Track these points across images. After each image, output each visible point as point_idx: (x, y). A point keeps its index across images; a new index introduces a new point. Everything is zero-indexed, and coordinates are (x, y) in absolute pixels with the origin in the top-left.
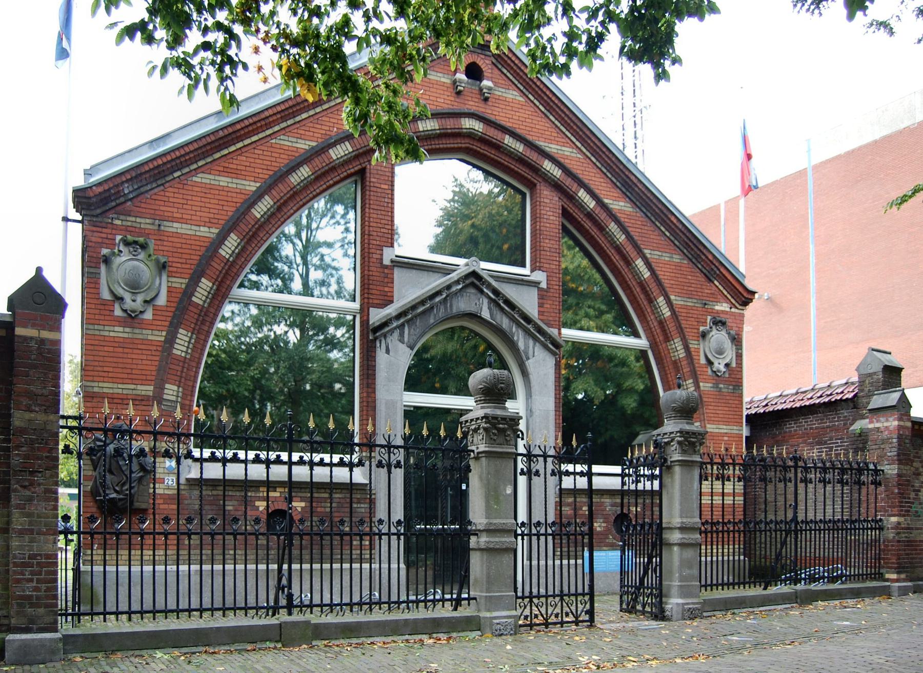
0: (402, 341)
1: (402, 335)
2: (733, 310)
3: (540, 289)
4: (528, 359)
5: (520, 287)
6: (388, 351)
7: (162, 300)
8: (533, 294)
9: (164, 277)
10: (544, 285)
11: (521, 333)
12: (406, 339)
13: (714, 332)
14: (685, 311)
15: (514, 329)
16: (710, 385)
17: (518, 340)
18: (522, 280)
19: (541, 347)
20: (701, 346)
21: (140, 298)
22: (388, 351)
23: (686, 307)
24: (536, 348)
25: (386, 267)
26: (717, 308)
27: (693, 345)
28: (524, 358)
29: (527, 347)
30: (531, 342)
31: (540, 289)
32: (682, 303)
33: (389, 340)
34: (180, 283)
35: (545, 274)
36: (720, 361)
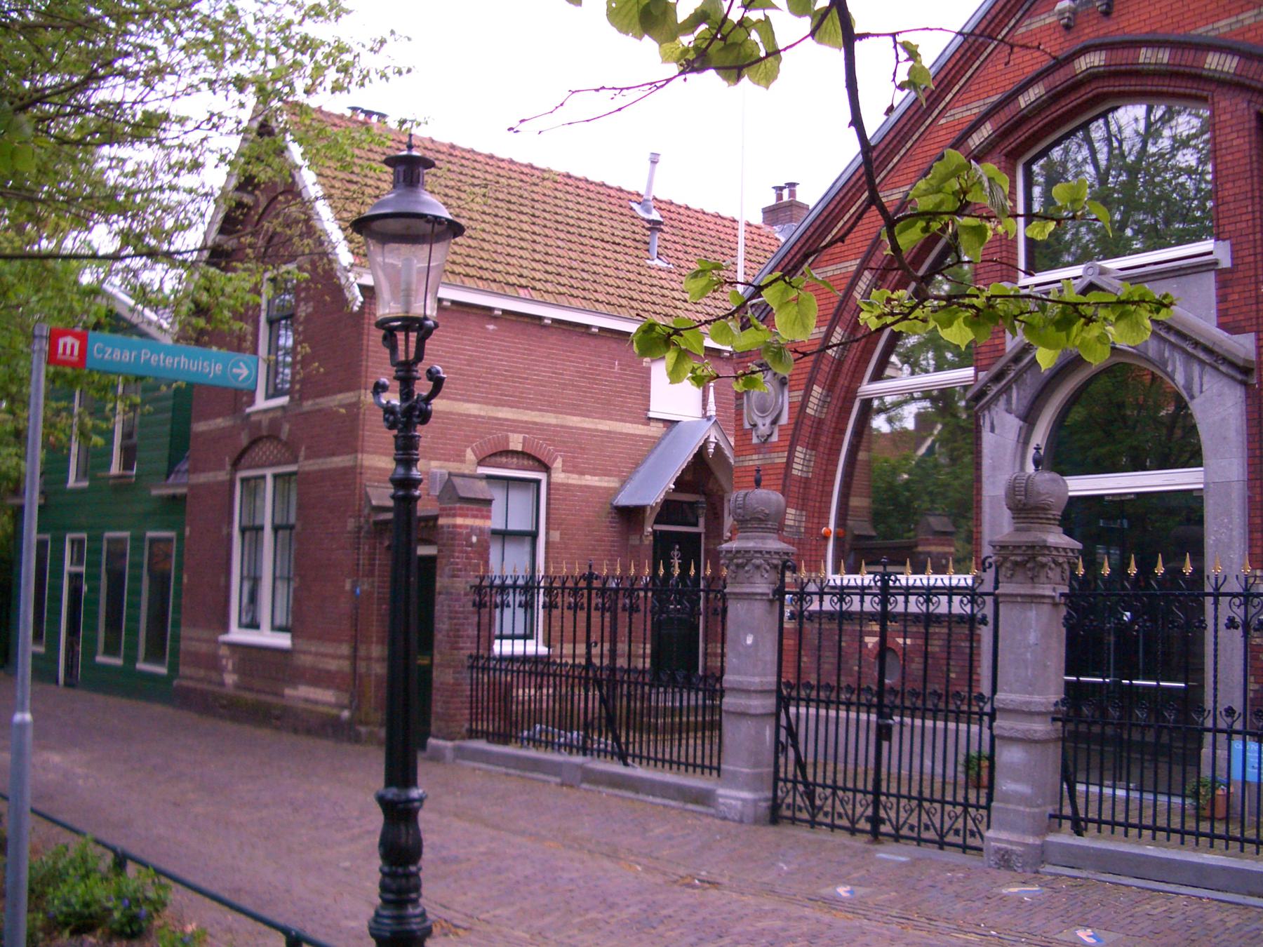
0: (1009, 411)
1: (1009, 401)
3: (1221, 273)
4: (1192, 397)
5: (1184, 279)
6: (992, 430)
7: (784, 420)
8: (1207, 284)
9: (786, 393)
10: (1226, 263)
12: (1014, 406)
15: (1167, 354)
17: (1174, 371)
18: (1180, 269)
19: (1214, 373)
21: (768, 421)
22: (992, 430)
24: (1205, 379)
28: (1187, 398)
30: (1196, 369)
31: (1221, 273)
33: (993, 412)
34: (798, 395)
35: (1227, 243)
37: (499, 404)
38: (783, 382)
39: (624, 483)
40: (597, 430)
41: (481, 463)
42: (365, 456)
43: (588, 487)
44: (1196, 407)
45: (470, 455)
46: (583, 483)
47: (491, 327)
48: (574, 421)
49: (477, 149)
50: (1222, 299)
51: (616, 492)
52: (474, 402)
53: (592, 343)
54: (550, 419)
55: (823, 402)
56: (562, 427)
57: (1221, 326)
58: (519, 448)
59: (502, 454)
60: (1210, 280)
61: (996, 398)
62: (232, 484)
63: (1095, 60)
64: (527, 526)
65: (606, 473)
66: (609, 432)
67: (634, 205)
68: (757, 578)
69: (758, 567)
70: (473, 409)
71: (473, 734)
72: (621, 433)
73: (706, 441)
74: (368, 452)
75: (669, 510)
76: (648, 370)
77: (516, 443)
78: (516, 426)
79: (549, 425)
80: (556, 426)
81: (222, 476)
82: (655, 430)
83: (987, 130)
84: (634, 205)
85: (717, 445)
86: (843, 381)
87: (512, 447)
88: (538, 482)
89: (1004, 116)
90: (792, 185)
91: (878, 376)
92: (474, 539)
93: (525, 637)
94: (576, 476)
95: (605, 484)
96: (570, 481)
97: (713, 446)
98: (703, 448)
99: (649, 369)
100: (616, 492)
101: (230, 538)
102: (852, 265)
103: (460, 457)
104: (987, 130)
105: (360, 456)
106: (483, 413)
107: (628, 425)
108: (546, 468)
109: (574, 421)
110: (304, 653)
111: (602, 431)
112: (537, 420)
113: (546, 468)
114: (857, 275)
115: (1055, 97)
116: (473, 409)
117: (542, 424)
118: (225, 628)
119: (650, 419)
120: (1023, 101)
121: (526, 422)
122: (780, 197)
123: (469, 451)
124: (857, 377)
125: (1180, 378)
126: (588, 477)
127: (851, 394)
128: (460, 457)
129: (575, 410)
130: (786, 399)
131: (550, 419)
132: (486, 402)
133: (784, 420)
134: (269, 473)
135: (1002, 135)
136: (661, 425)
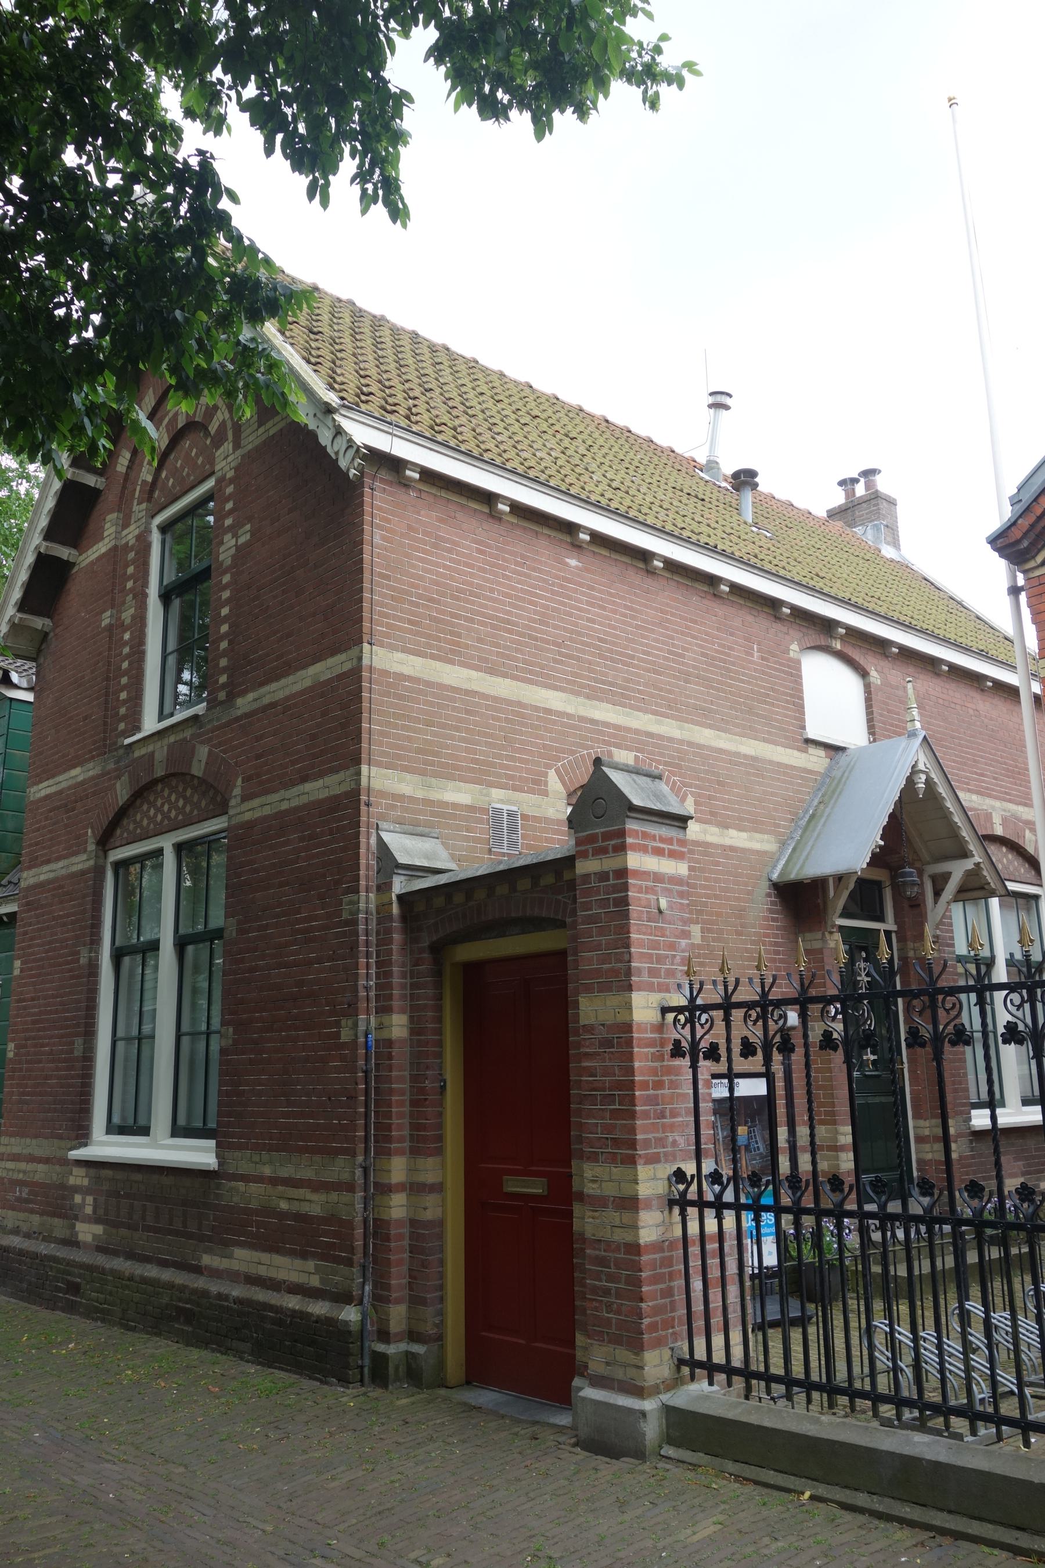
37: (594, 695)
40: (737, 754)
42: (374, 770)
43: (732, 848)
46: (728, 842)
47: (573, 562)
48: (706, 736)
52: (555, 688)
53: (720, 610)
54: (669, 728)
56: (690, 744)
62: (98, 872)
65: (755, 826)
66: (754, 759)
70: (555, 700)
72: (771, 762)
73: (914, 771)
74: (379, 765)
79: (671, 739)
80: (681, 742)
81: (80, 862)
85: (929, 782)
90: (869, 474)
94: (714, 829)
95: (757, 846)
96: (710, 839)
97: (923, 777)
98: (910, 781)
99: (799, 662)
101: (93, 970)
105: (364, 768)
106: (570, 710)
107: (780, 749)
109: (706, 736)
110: (245, 1178)
111: (745, 756)
112: (654, 728)
116: (555, 700)
117: (660, 737)
118: (82, 1135)
119: (808, 741)
121: (637, 732)
122: (850, 493)
123: (552, 773)
126: (732, 832)
129: (704, 717)
131: (669, 728)
134: (167, 843)
136: (822, 753)
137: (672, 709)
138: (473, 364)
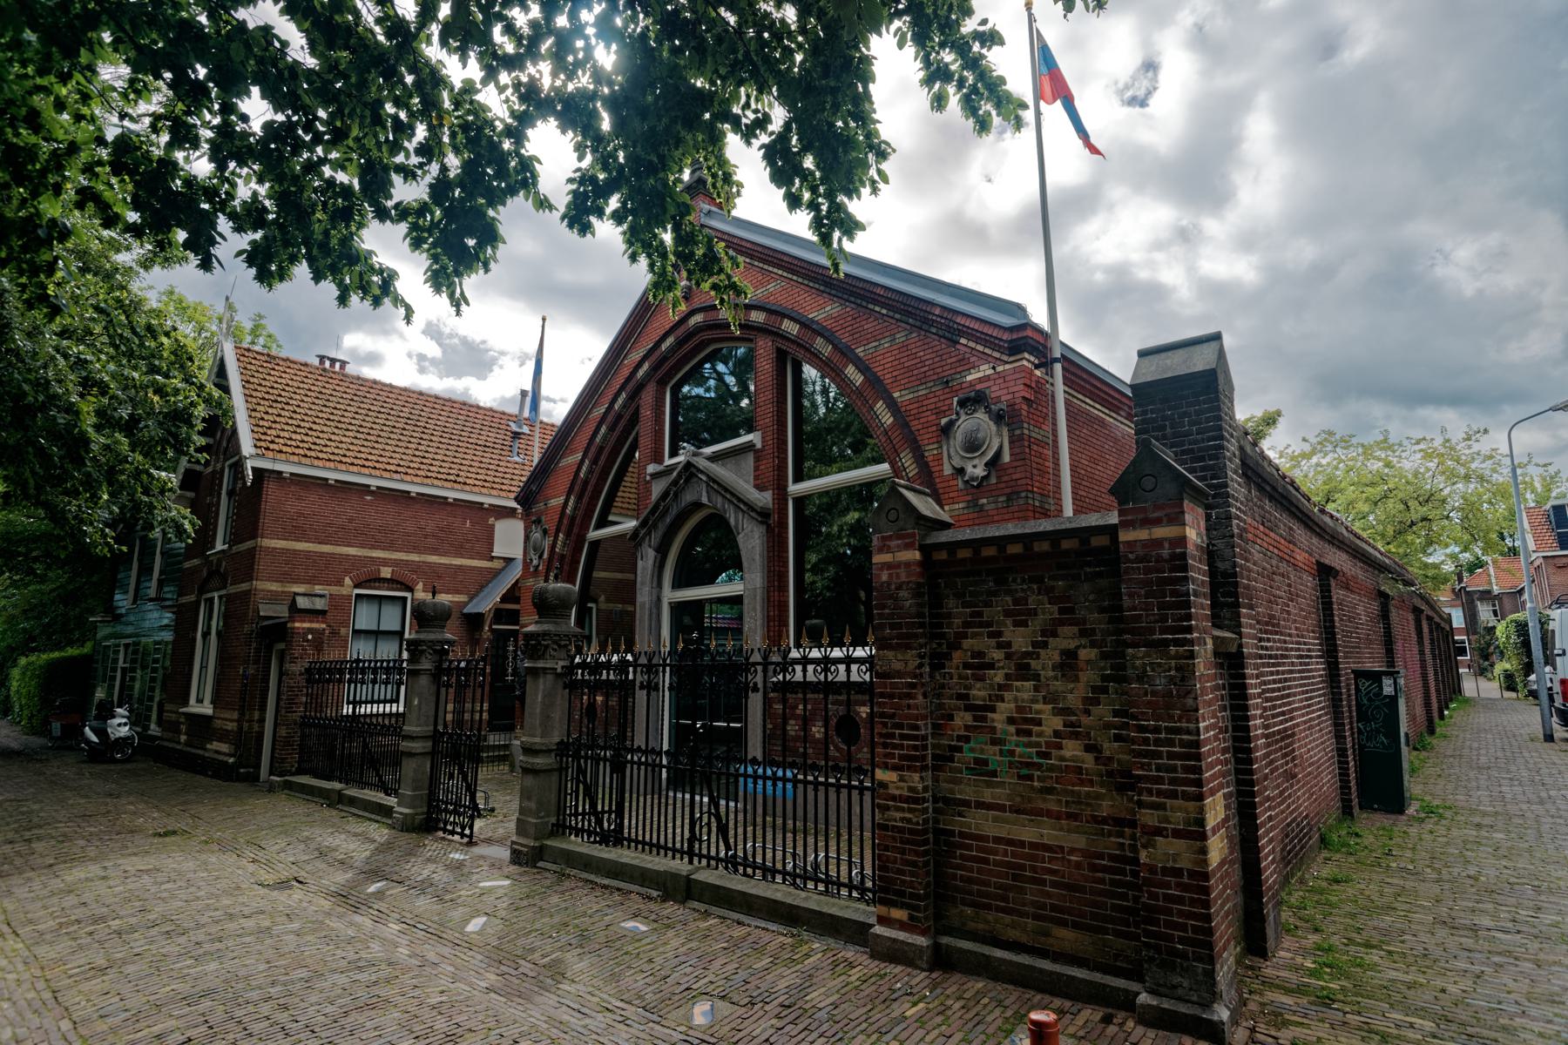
2: (1000, 369)
7: (545, 556)
10: (759, 446)
11: (732, 508)
13: (963, 417)
14: (916, 405)
16: (961, 505)
20: (945, 448)
23: (917, 400)
25: (648, 482)
26: (969, 378)
27: (930, 451)
29: (737, 523)
31: (757, 451)
32: (911, 396)
36: (976, 462)
37: (373, 547)
38: (545, 532)
39: (471, 599)
41: (356, 586)
44: (740, 539)
45: (347, 581)
49: (394, 383)
50: (756, 469)
51: (466, 604)
54: (414, 557)
55: (564, 544)
57: (757, 487)
58: (389, 576)
59: (376, 581)
60: (750, 458)
61: (643, 538)
62: (198, 603)
63: (698, 318)
64: (397, 627)
65: (457, 592)
67: (511, 424)
68: (423, 659)
69: (424, 651)
70: (352, 551)
71: (300, 772)
75: (500, 615)
76: (492, 528)
77: (386, 573)
78: (385, 562)
81: (193, 598)
82: (497, 564)
83: (646, 366)
84: (511, 424)
86: (575, 530)
87: (383, 575)
88: (405, 599)
89: (654, 358)
91: (603, 523)
92: (310, 637)
93: (391, 701)
100: (466, 604)
101: (194, 640)
102: (579, 456)
103: (340, 583)
104: (646, 366)
108: (411, 590)
112: (405, 558)
113: (411, 590)
114: (582, 461)
115: (680, 343)
116: (352, 551)
120: (664, 347)
124: (585, 528)
125: (732, 522)
127: (581, 539)
128: (340, 583)
129: (435, 551)
130: (547, 543)
131: (414, 557)
132: (362, 546)
133: (545, 556)
134: (216, 595)
135: (655, 368)
137: (415, 549)
138: (391, 386)
